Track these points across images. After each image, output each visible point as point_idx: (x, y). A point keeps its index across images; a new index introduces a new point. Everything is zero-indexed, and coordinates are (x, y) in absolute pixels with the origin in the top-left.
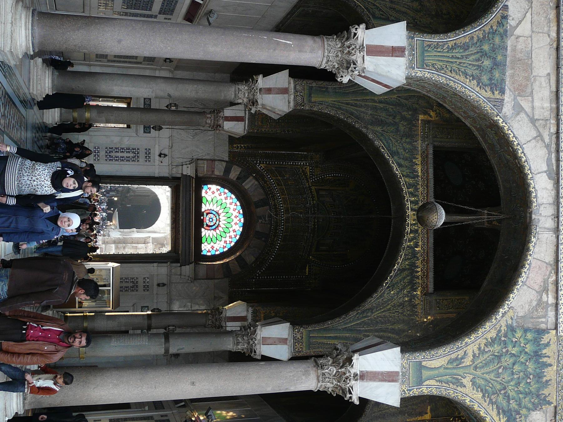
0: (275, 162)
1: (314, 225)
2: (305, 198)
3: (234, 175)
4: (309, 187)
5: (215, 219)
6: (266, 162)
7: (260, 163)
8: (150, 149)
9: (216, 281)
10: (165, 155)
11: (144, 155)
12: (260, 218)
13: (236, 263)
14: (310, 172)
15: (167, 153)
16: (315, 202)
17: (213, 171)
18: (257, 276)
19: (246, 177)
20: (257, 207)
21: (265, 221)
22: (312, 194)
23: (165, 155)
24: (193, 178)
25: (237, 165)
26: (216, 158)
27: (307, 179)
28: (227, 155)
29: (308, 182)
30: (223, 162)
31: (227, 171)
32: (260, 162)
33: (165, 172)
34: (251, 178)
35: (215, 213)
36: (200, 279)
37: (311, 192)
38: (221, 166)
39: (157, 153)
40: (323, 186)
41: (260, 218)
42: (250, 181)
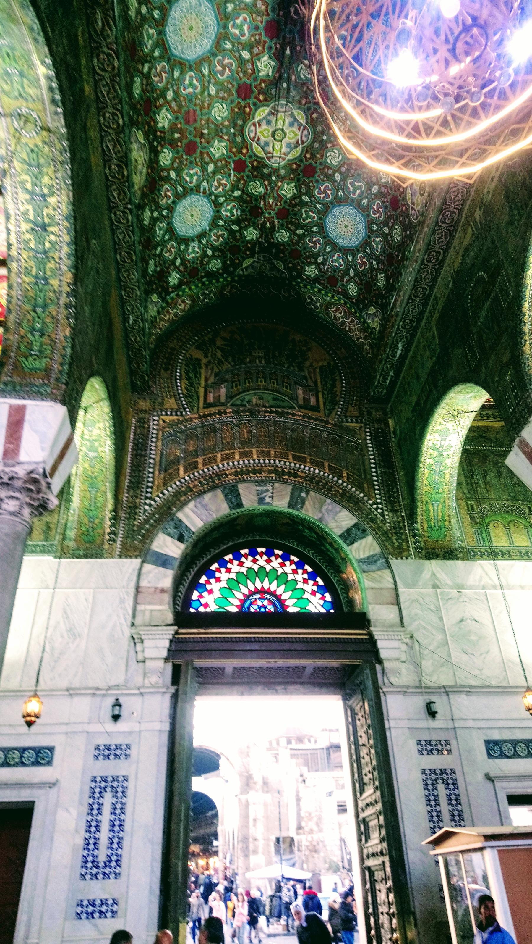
0: (150, 472)
1: (271, 412)
2: (222, 426)
3: (174, 548)
4: (200, 417)
5: (259, 603)
6: (148, 487)
7: (150, 498)
8: (98, 748)
9: (399, 583)
10: (117, 704)
11: (112, 762)
12: (261, 501)
13: (356, 545)
14: (171, 415)
15: (111, 701)
16: (228, 410)
17: (163, 591)
18: (377, 508)
19: (179, 524)
20: (240, 505)
21: (267, 491)
22: (215, 414)
23: (117, 704)
24: (177, 633)
25: (152, 542)
26: (133, 584)
27: (187, 420)
28: (128, 560)
29: (191, 419)
30: (144, 570)
31: (163, 561)
32: (147, 498)
33: (160, 705)
34: (180, 515)
35: (248, 602)
36: (401, 618)
37: (210, 415)
38: (151, 575)
39: (110, 726)
40: (198, 397)
41: (261, 501)
42: (187, 516)
